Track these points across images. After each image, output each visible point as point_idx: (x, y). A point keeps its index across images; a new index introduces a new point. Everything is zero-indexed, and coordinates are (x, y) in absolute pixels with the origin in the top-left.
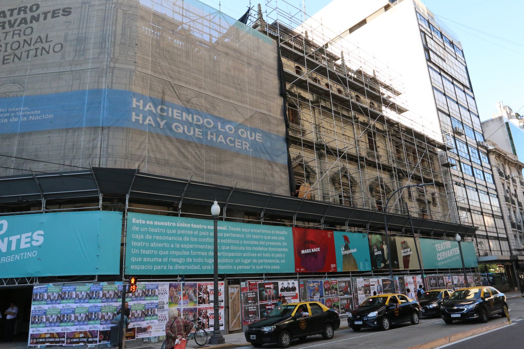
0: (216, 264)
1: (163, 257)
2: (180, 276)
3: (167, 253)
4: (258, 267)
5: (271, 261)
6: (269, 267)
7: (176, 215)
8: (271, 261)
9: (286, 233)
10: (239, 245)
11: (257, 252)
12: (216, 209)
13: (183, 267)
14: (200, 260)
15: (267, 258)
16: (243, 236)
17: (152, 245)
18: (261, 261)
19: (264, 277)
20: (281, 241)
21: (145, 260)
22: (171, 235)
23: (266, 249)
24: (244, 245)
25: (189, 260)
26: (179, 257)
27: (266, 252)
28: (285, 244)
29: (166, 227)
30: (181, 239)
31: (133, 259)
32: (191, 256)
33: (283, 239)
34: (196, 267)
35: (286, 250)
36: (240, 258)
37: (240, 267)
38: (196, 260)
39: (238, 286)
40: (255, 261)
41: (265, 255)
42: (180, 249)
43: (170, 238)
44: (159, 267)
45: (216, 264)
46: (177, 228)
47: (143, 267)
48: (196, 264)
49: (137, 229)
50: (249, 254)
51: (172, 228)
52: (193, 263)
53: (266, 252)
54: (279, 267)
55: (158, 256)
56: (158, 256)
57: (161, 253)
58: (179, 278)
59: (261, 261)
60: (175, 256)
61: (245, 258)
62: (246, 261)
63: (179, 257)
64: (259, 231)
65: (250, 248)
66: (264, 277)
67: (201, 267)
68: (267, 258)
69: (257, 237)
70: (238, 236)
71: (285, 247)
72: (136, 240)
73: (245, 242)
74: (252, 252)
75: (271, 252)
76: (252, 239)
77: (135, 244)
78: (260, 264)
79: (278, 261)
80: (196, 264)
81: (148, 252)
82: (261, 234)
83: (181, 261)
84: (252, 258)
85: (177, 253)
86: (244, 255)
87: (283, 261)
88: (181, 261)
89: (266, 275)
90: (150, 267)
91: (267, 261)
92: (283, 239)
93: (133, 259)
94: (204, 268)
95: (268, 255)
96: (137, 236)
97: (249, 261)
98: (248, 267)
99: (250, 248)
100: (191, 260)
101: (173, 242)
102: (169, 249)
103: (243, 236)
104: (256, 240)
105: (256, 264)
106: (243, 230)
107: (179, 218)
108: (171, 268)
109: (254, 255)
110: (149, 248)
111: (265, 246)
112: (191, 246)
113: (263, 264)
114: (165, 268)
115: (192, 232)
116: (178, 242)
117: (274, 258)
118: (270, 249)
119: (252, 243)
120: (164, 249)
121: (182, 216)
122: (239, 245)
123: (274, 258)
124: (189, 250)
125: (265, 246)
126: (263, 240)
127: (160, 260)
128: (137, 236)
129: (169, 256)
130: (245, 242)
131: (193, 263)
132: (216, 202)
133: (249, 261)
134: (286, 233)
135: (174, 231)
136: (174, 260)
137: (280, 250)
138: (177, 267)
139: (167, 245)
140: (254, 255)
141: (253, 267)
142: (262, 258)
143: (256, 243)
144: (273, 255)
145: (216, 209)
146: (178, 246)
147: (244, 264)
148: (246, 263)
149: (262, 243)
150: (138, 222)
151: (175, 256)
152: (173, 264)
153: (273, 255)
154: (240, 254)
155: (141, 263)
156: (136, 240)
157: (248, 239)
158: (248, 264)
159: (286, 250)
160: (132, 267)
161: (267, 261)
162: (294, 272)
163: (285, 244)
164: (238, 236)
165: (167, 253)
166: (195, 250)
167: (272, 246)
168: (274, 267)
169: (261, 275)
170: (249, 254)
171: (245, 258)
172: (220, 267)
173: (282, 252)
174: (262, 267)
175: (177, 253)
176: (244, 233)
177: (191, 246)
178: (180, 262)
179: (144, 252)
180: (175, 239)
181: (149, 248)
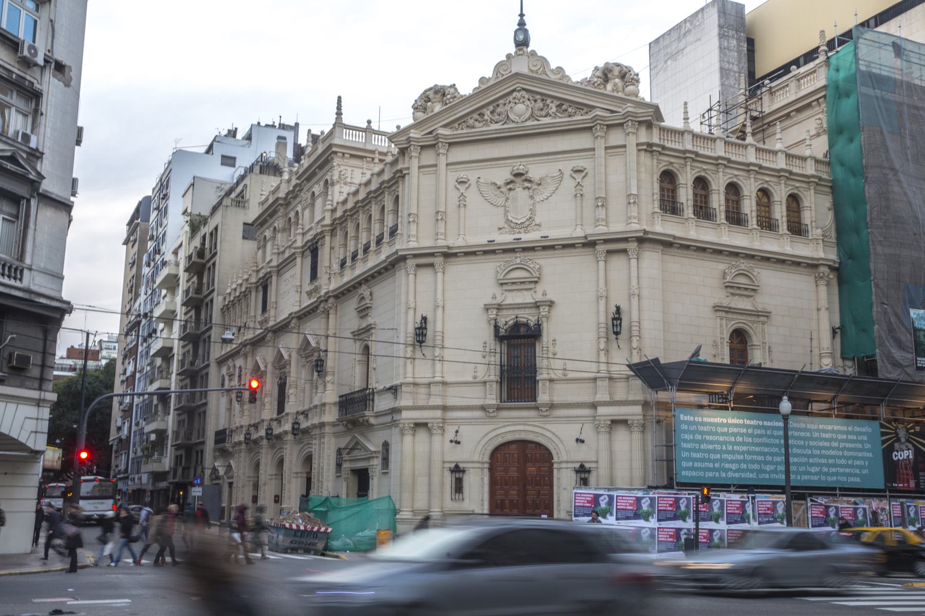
0: (787, 472)
1: (714, 461)
2: (734, 485)
3: (718, 456)
4: (829, 479)
5: (847, 470)
6: (845, 479)
7: (726, 408)
8: (847, 470)
9: (870, 430)
10: (803, 447)
11: (828, 457)
12: (786, 406)
13: (737, 475)
14: (756, 466)
15: (842, 466)
16: (808, 434)
17: (702, 447)
18: (834, 470)
19: (838, 492)
20: (861, 442)
21: (696, 465)
22: (723, 434)
23: (840, 453)
24: (810, 447)
25: (744, 466)
26: (732, 462)
27: (840, 458)
28: (868, 446)
29: (717, 425)
30: (733, 439)
31: (684, 464)
32: (745, 461)
33: (865, 438)
34: (751, 476)
35: (870, 455)
36: (805, 464)
37: (806, 477)
38: (751, 467)
39: (803, 502)
40: (825, 469)
41: (839, 462)
42: (733, 452)
43: (721, 439)
44: (711, 474)
45: (787, 472)
46: (728, 425)
47: (694, 474)
48: (752, 471)
49: (686, 427)
50: (816, 460)
51: (722, 425)
52: (747, 470)
53: (840, 458)
54: (858, 480)
55: (709, 460)
56: (709, 460)
57: (712, 456)
58: (732, 489)
59: (834, 470)
60: (727, 461)
61: (812, 465)
62: (814, 470)
63: (732, 462)
64: (830, 428)
65: (818, 452)
66: (838, 492)
67: (757, 475)
68: (842, 466)
69: (827, 436)
70: (802, 434)
71: (868, 451)
72: (686, 441)
73: (811, 443)
74: (821, 456)
75: (847, 458)
76: (821, 439)
77: (684, 445)
78: (833, 474)
79: (858, 471)
80: (752, 471)
81: (698, 455)
82: (833, 431)
83: (734, 466)
84: (821, 465)
85: (730, 457)
86: (811, 461)
87: (865, 471)
88: (734, 466)
89: (841, 489)
90: (701, 474)
91: (841, 470)
92: (865, 438)
93: (684, 464)
94: (761, 476)
95: (843, 462)
96: (686, 436)
97: (817, 469)
98: (816, 478)
99: (818, 452)
100: (745, 466)
101: (725, 443)
102: (721, 452)
103: (808, 434)
104: (826, 440)
105: (827, 474)
106: (809, 426)
107: (730, 412)
108: (724, 475)
109: (824, 461)
110: (699, 451)
111: (838, 449)
112: (745, 448)
113: (836, 474)
114: (717, 475)
115: (745, 431)
116: (730, 443)
117: (852, 466)
118: (846, 453)
119: (821, 444)
120: (714, 451)
121: (733, 409)
122: (803, 447)
123: (852, 466)
124: (743, 453)
125: (838, 449)
126: (836, 440)
127: (711, 465)
128: (686, 436)
129: (722, 461)
130: (811, 443)
131: (747, 470)
132: (785, 398)
133: (817, 469)
134: (870, 430)
135: (726, 430)
136: (727, 466)
137: (860, 454)
138: (730, 474)
139: (718, 447)
140: (824, 461)
141: (823, 478)
142: (835, 465)
143: (827, 444)
144: (850, 462)
145: (786, 406)
146: (730, 448)
147: (810, 473)
148: (813, 471)
149: (835, 444)
150: (686, 418)
151: (727, 461)
152: (726, 471)
153: (850, 462)
154: (804, 460)
155: (693, 469)
156: (686, 441)
157: (816, 439)
158: (816, 474)
159: (870, 455)
160: (683, 473)
161: (841, 470)
162: (882, 487)
163: (868, 446)
164: (802, 434)
165: (718, 456)
166: (749, 453)
167: (849, 450)
168: (852, 479)
169: (834, 489)
170: (816, 460)
171: (812, 465)
172: (792, 477)
173: (863, 458)
174: (835, 478)
175: (730, 457)
176: (810, 431)
177: (745, 448)
178: (734, 468)
179: (694, 455)
180: (727, 438)
181: (699, 451)
